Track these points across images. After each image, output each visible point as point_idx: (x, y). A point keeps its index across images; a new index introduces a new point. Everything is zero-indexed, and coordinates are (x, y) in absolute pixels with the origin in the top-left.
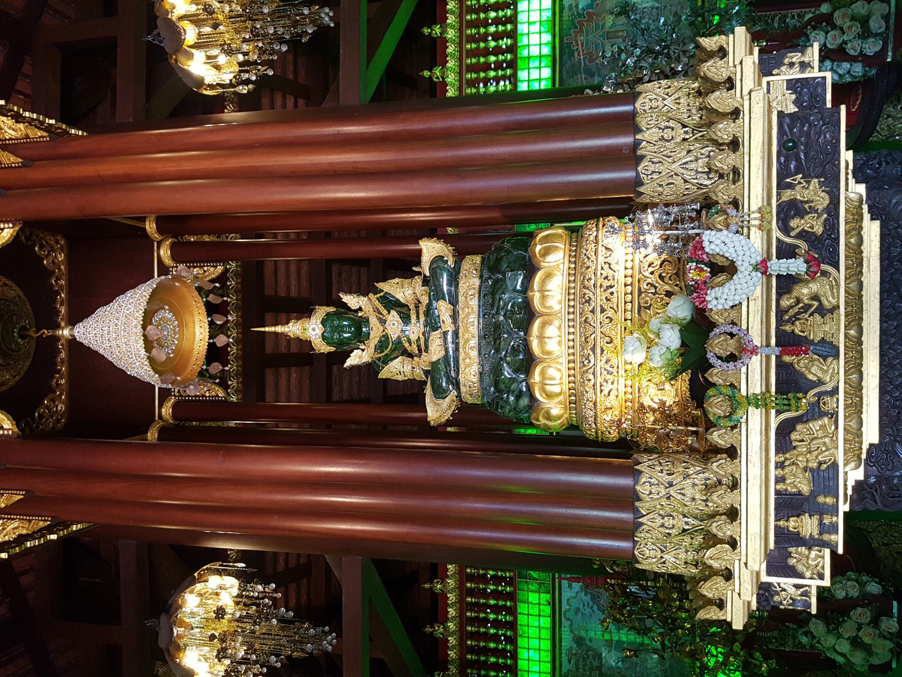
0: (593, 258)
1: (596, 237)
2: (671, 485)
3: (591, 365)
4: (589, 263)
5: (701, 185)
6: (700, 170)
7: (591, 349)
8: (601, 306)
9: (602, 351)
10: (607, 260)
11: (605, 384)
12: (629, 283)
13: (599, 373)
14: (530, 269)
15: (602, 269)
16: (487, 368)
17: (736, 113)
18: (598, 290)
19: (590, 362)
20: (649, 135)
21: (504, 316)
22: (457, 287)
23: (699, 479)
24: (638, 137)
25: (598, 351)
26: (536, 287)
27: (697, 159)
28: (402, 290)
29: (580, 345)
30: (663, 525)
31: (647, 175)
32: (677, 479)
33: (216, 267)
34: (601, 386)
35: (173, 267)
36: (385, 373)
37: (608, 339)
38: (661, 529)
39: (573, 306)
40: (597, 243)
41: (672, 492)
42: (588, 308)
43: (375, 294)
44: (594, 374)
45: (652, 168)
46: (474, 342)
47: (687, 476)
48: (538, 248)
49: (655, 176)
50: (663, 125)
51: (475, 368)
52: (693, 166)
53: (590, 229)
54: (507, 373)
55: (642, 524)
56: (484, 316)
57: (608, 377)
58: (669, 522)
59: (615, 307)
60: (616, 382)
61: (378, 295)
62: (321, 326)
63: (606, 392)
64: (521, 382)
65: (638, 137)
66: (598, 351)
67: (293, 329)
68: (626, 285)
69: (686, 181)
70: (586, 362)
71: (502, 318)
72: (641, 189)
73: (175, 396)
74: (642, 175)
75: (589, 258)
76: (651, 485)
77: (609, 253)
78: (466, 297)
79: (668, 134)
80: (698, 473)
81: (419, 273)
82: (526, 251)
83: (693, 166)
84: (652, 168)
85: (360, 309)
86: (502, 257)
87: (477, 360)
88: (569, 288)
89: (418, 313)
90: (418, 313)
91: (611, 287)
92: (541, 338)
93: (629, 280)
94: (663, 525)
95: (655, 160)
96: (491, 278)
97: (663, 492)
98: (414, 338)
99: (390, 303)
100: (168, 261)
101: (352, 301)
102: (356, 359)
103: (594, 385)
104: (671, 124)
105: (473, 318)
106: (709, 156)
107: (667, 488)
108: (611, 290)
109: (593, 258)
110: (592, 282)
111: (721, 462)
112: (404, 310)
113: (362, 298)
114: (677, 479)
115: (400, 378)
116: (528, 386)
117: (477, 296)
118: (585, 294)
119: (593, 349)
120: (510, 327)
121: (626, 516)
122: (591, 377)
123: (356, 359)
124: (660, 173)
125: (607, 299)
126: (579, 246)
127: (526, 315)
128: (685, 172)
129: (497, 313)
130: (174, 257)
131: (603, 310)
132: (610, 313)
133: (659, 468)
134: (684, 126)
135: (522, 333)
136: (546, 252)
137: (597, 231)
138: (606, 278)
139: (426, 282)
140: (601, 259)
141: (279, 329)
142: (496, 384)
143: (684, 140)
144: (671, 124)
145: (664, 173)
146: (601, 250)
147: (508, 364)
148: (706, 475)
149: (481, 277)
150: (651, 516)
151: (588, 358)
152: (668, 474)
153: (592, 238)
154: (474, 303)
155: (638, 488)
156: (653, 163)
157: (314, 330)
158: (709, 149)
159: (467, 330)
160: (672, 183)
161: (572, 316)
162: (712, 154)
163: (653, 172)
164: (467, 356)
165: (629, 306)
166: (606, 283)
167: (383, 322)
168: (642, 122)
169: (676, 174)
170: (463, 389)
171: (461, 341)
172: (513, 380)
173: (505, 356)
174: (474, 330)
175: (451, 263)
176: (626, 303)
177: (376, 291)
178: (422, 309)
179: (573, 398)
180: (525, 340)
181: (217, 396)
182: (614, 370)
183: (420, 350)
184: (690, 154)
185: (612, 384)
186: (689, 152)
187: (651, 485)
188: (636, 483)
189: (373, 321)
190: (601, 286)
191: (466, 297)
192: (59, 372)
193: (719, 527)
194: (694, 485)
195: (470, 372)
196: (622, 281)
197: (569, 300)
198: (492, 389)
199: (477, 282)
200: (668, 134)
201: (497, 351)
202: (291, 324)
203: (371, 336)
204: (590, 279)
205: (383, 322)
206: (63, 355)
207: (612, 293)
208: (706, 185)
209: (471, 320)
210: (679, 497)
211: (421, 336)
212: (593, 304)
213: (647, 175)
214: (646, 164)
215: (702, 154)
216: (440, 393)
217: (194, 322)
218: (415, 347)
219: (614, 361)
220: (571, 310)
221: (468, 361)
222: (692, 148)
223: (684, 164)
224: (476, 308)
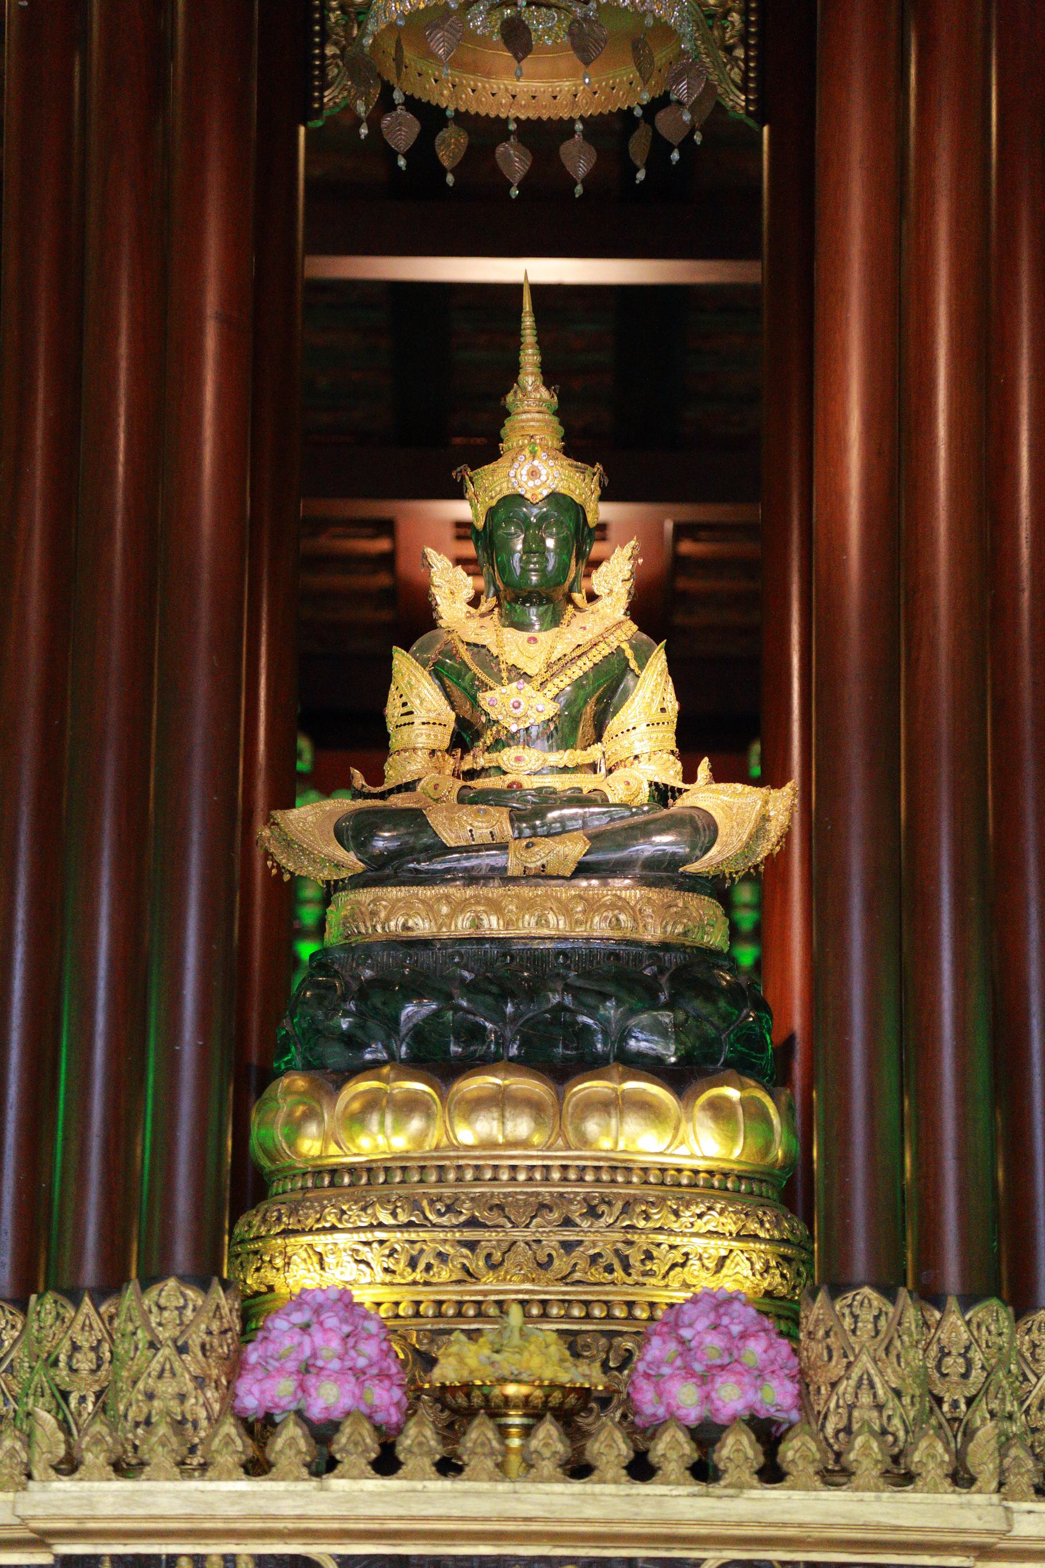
0: (701, 1226)
1: (755, 1237)
3: (432, 1217)
4: (687, 1216)
5: (825, 1418)
6: (856, 1413)
7: (473, 1217)
8: (580, 1243)
9: (472, 1246)
10: (693, 1261)
11: (387, 1252)
12: (638, 1313)
13: (413, 1236)
14: (682, 1078)
15: (672, 1247)
16: (426, 957)
17: (961, 1477)
18: (618, 1236)
19: (440, 1214)
20: (955, 1326)
21: (561, 1007)
23: (195, 1408)
24: (953, 1304)
25: (469, 1235)
26: (630, 1085)
27: (880, 1407)
29: (483, 1194)
30: (75, 1348)
31: (850, 1306)
32: (193, 1362)
34: (382, 1242)
36: (405, 666)
37: (497, 1256)
38: (66, 1345)
39: (581, 1179)
40: (739, 1237)
41: (166, 1351)
42: (576, 1211)
44: (410, 1224)
45: (867, 1316)
46: (493, 925)
47: (200, 1382)
48: (733, 1094)
49: (848, 1323)
50: (977, 1356)
51: (423, 927)
52: (865, 1399)
53: (777, 1225)
54: (411, 1011)
55: (77, 1304)
56: (563, 952)
57: (403, 1260)
58: (85, 1362)
59: (577, 1276)
60: (388, 1278)
61: (629, 653)
63: (365, 1253)
64: (387, 1048)
65: (953, 1304)
66: (469, 1235)
68: (630, 1305)
69: (834, 1385)
70: (439, 1206)
71: (555, 999)
72: (821, 1296)
74: (850, 1295)
75: (700, 1216)
76: (181, 1309)
77: (712, 1265)
78: (612, 906)
79: (954, 1365)
80: (207, 1405)
81: (689, 776)
82: (728, 1064)
83: (865, 1399)
84: (867, 1316)
85: (592, 597)
86: (714, 1002)
87: (445, 933)
88: (629, 1170)
89: (577, 769)
90: (577, 769)
91: (626, 1268)
92: (500, 1102)
93: (641, 1314)
94: (75, 1348)
95: (883, 1323)
96: (661, 971)
97: (164, 1334)
98: (506, 757)
99: (601, 694)
101: (615, 576)
103: (381, 1225)
104: (977, 1375)
105: (557, 924)
106: (884, 1432)
107: (175, 1341)
108: (617, 1266)
109: (701, 1226)
110: (641, 1224)
111: (239, 1442)
112: (585, 728)
113: (623, 602)
114: (193, 1362)
115: (393, 711)
116: (377, 1064)
117: (618, 934)
118: (609, 1204)
119: (472, 1223)
120: (533, 1017)
121: (90, 1272)
122: (403, 1218)
124: (854, 1331)
125: (594, 1259)
126: (732, 1196)
127: (560, 1056)
128: (852, 1382)
129: (568, 988)
131: (568, 1246)
132: (562, 1264)
133: (215, 1327)
134: (970, 1401)
135: (514, 1051)
136: (718, 1109)
137: (771, 1241)
138: (649, 1256)
139: (663, 794)
140: (696, 1245)
141: (530, 357)
142: (381, 983)
143: (939, 1401)
144: (977, 1375)
145: (852, 1339)
146: (718, 1248)
147: (436, 1014)
148: (204, 1423)
149: (665, 946)
150: (97, 1323)
151: (449, 1209)
152: (203, 1347)
153: (753, 1226)
154: (599, 927)
155: (172, 1283)
156: (877, 1318)
158: (901, 1434)
159: (526, 906)
160: (830, 1358)
161: (556, 1175)
162: (890, 1438)
163: (856, 1318)
164: (460, 907)
165: (576, 1312)
166: (635, 1257)
168: (991, 1314)
169: (849, 1365)
170: (366, 895)
171: (494, 891)
172: (392, 1023)
173: (457, 1008)
174: (527, 926)
176: (587, 1303)
178: (586, 782)
179: (346, 1180)
180: (497, 1058)
182: (419, 1276)
183: (471, 774)
184: (891, 1395)
185: (387, 1270)
186: (898, 1393)
187: (181, 1309)
188: (183, 1279)
190: (630, 1243)
191: (612, 906)
193: (98, 1440)
194: (182, 1397)
196: (641, 1296)
197: (598, 1169)
198: (368, 973)
199: (652, 933)
200: (954, 1365)
201: (470, 989)
203: (510, 633)
204: (647, 1218)
207: (609, 1269)
208: (823, 1426)
209: (551, 917)
210: (155, 1366)
211: (509, 779)
212: (585, 1224)
213: (850, 1306)
214: (875, 1303)
215: (889, 1418)
216: (354, 832)
218: (482, 761)
220: (572, 1175)
221: (445, 910)
222: (906, 1400)
223: (872, 1385)
224: (580, 931)
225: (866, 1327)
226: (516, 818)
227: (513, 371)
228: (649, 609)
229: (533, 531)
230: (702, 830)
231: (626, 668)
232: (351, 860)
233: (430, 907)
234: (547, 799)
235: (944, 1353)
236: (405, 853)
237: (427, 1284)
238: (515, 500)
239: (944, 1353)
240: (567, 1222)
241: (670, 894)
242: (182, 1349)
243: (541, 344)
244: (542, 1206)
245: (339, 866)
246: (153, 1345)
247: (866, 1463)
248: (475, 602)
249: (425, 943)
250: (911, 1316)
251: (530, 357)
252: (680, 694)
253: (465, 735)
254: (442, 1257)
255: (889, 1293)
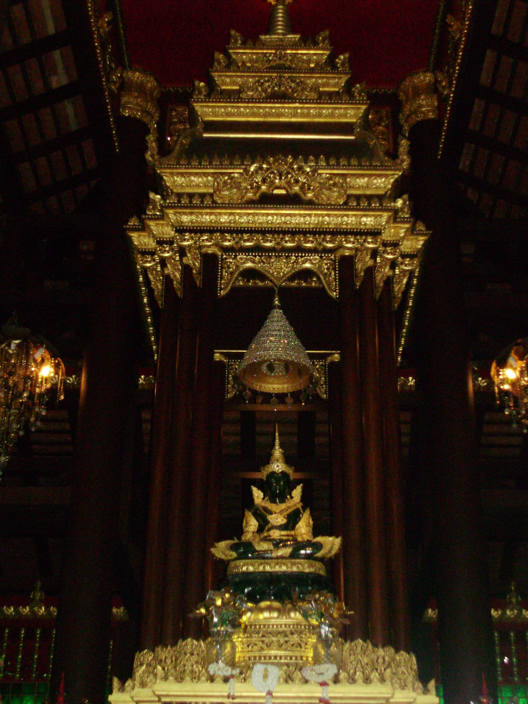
2: (192, 654)
20: (381, 652)
22: (304, 558)
28: (304, 528)
33: (325, 394)
35: (325, 362)
37: (269, 644)
43: (302, 507)
46: (268, 568)
49: (355, 648)
57: (246, 646)
61: (301, 509)
62: (280, 471)
67: (278, 452)
73: (229, 362)
76: (192, 646)
79: (380, 660)
83: (359, 666)
85: (292, 497)
87: (257, 570)
92: (270, 609)
98: (271, 533)
100: (329, 359)
101: (297, 492)
102: (258, 494)
105: (284, 568)
119: (263, 636)
123: (258, 494)
125: (293, 645)
130: (332, 363)
131: (286, 642)
141: (277, 442)
156: (362, 647)
157: (278, 466)
163: (357, 647)
167: (281, 512)
175: (319, 554)
177: (304, 508)
181: (228, 393)
189: (283, 506)
192: (248, 281)
195: (247, 567)
202: (281, 450)
205: (281, 512)
206: (260, 284)
212: (291, 636)
217: (284, 383)
219: (255, 648)
223: (361, 662)
225: (359, 649)
226: (274, 545)
227: (274, 445)
228: (304, 499)
229: (278, 481)
230: (318, 547)
231: (300, 513)
232: (234, 554)
233: (252, 565)
234: (281, 541)
235: (378, 658)
236: (246, 550)
237: (251, 651)
238: (273, 473)
239: (378, 658)
240: (286, 636)
241: (311, 561)
242: (192, 654)
243: (280, 440)
244: (280, 633)
245: (231, 556)
246: (185, 654)
247: (359, 678)
248: (263, 499)
249: (251, 573)
250: (370, 647)
251: (277, 442)
252: (313, 520)
253: (260, 530)
254: (256, 645)
255: (365, 641)
